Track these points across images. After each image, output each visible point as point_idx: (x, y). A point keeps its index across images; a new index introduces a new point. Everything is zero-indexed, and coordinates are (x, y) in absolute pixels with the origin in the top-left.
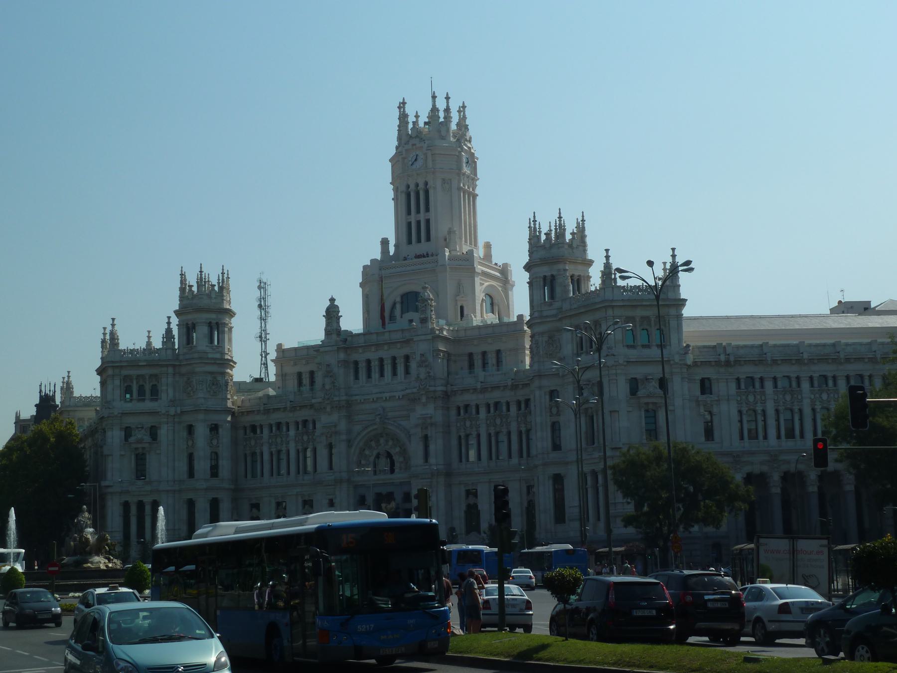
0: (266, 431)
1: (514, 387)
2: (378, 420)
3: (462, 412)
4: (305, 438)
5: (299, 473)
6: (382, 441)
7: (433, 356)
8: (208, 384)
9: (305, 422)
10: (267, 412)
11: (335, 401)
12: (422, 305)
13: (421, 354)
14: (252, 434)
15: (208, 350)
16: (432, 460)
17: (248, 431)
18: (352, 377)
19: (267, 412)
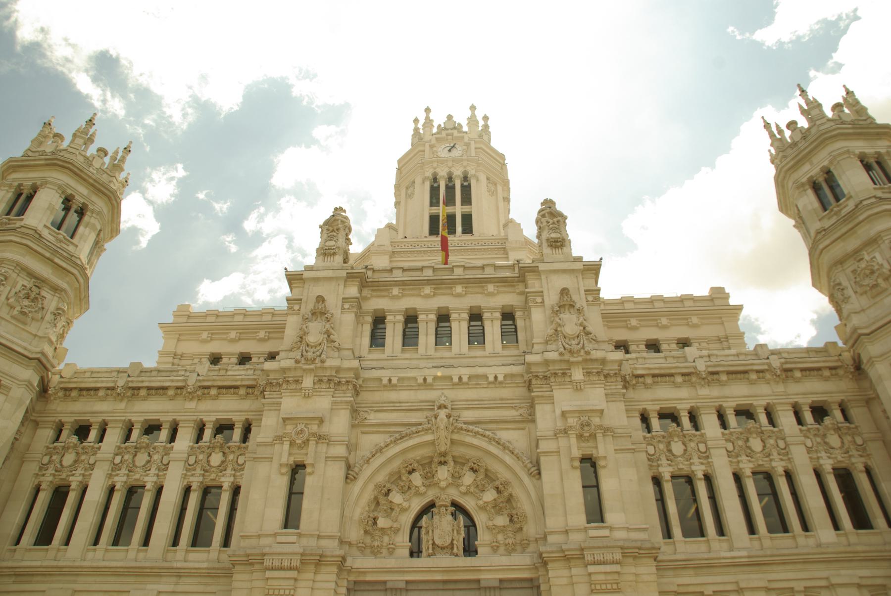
0: (113, 437)
1: (787, 372)
2: (443, 413)
3: (655, 423)
4: (216, 459)
5: (175, 542)
6: (443, 474)
7: (587, 301)
8: (14, 291)
9: (224, 428)
10: (134, 392)
11: (325, 368)
12: (551, 221)
13: (564, 292)
14: (75, 439)
15: (45, 233)
16: (611, 517)
17: (65, 433)
18: (366, 340)
19: (134, 392)
